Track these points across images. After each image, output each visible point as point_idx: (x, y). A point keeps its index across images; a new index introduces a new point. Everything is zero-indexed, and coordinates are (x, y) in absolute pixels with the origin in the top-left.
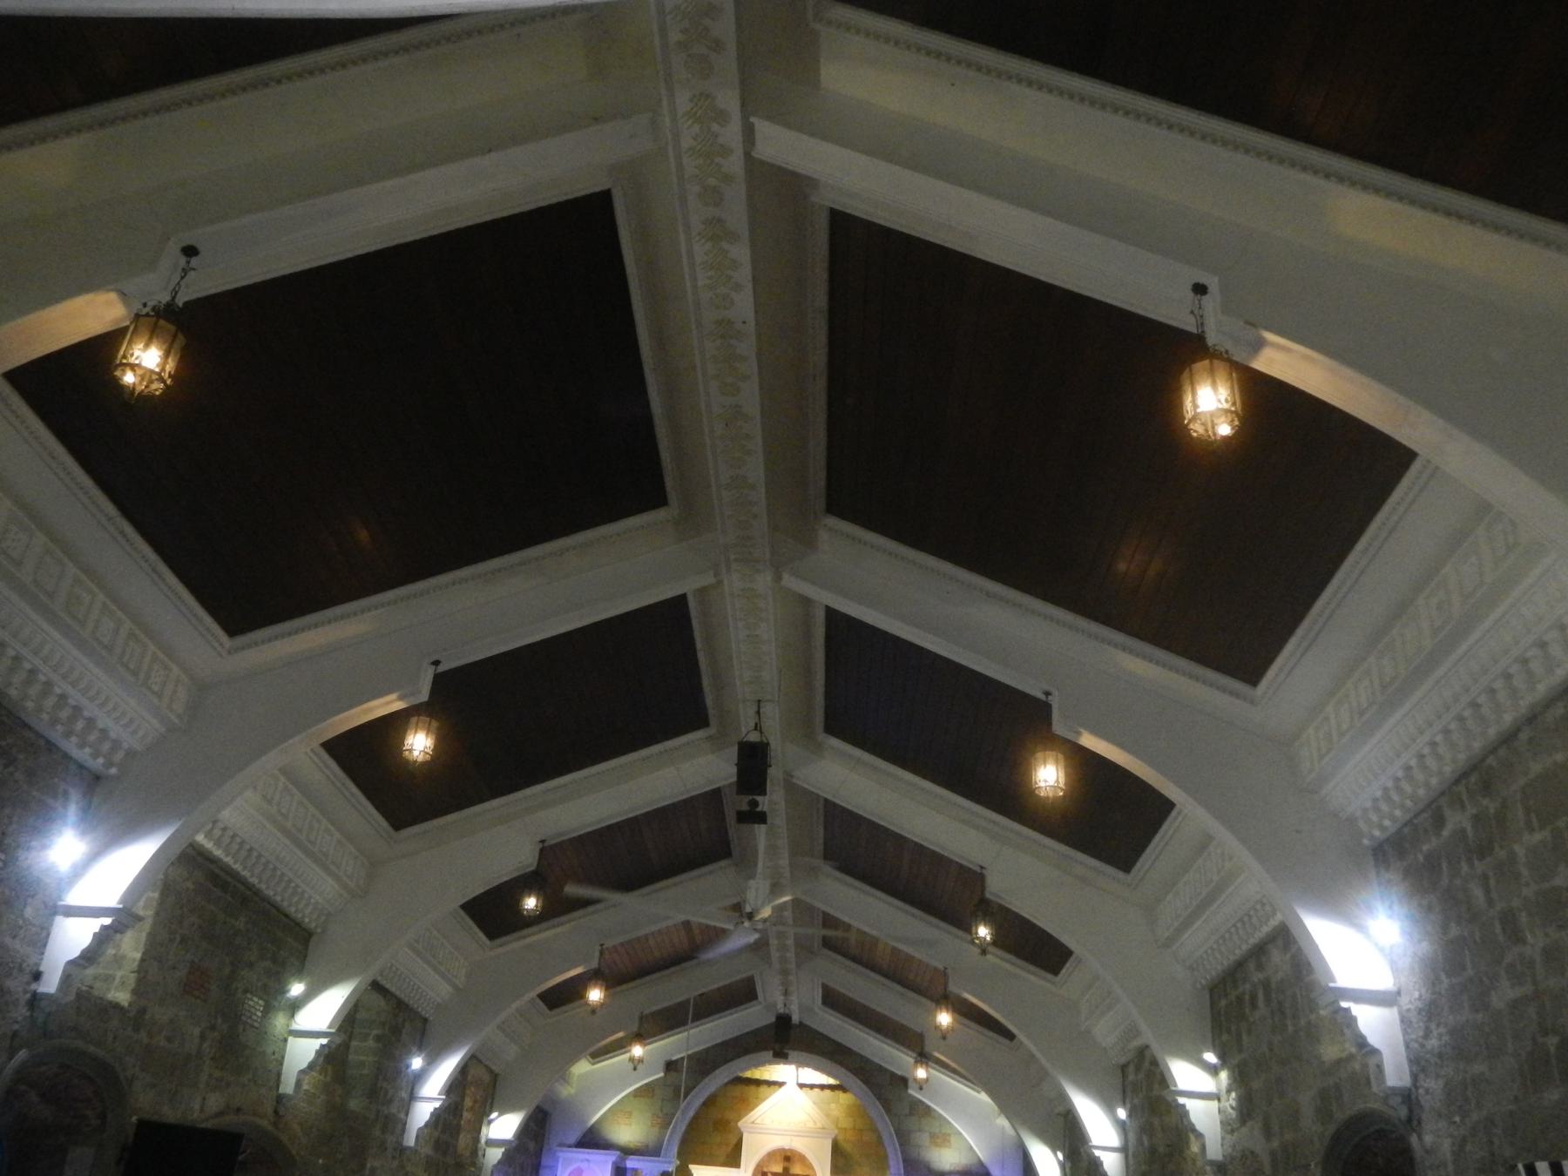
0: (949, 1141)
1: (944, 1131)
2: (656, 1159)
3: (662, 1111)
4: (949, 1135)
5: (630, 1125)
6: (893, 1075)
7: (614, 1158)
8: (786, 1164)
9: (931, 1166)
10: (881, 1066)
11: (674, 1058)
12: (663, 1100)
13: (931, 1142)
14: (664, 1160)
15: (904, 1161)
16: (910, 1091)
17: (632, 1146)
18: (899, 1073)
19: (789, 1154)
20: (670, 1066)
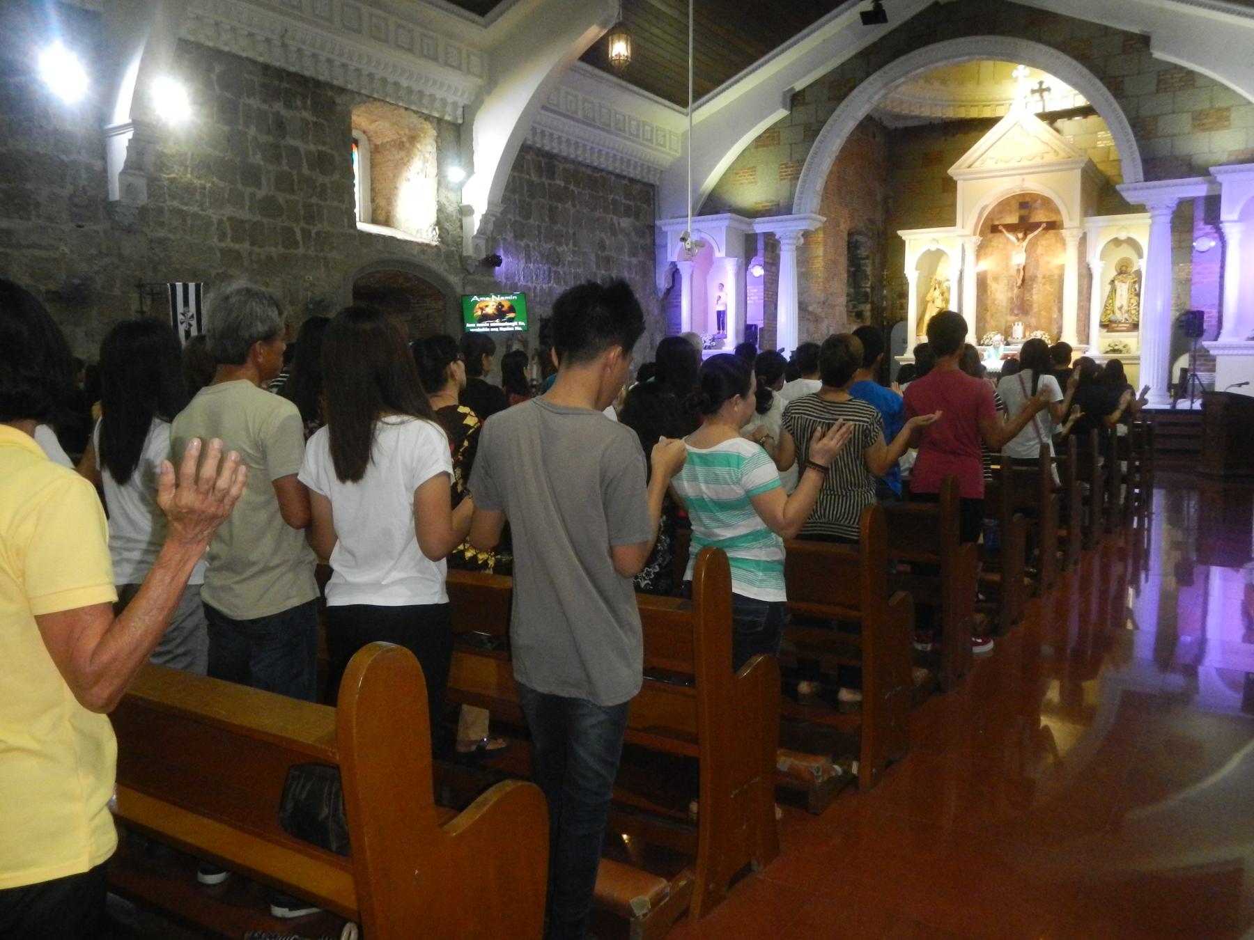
0: (1227, 119)
1: (1218, 105)
2: (789, 216)
3: (791, 160)
4: (1228, 109)
5: (756, 182)
6: (1128, 36)
7: (726, 223)
8: (1024, 212)
10: (1106, 28)
11: (799, 86)
12: (791, 144)
13: (1194, 126)
14: (797, 216)
16: (1157, 54)
17: (760, 207)
18: (1136, 30)
19: (1027, 199)
20: (795, 99)
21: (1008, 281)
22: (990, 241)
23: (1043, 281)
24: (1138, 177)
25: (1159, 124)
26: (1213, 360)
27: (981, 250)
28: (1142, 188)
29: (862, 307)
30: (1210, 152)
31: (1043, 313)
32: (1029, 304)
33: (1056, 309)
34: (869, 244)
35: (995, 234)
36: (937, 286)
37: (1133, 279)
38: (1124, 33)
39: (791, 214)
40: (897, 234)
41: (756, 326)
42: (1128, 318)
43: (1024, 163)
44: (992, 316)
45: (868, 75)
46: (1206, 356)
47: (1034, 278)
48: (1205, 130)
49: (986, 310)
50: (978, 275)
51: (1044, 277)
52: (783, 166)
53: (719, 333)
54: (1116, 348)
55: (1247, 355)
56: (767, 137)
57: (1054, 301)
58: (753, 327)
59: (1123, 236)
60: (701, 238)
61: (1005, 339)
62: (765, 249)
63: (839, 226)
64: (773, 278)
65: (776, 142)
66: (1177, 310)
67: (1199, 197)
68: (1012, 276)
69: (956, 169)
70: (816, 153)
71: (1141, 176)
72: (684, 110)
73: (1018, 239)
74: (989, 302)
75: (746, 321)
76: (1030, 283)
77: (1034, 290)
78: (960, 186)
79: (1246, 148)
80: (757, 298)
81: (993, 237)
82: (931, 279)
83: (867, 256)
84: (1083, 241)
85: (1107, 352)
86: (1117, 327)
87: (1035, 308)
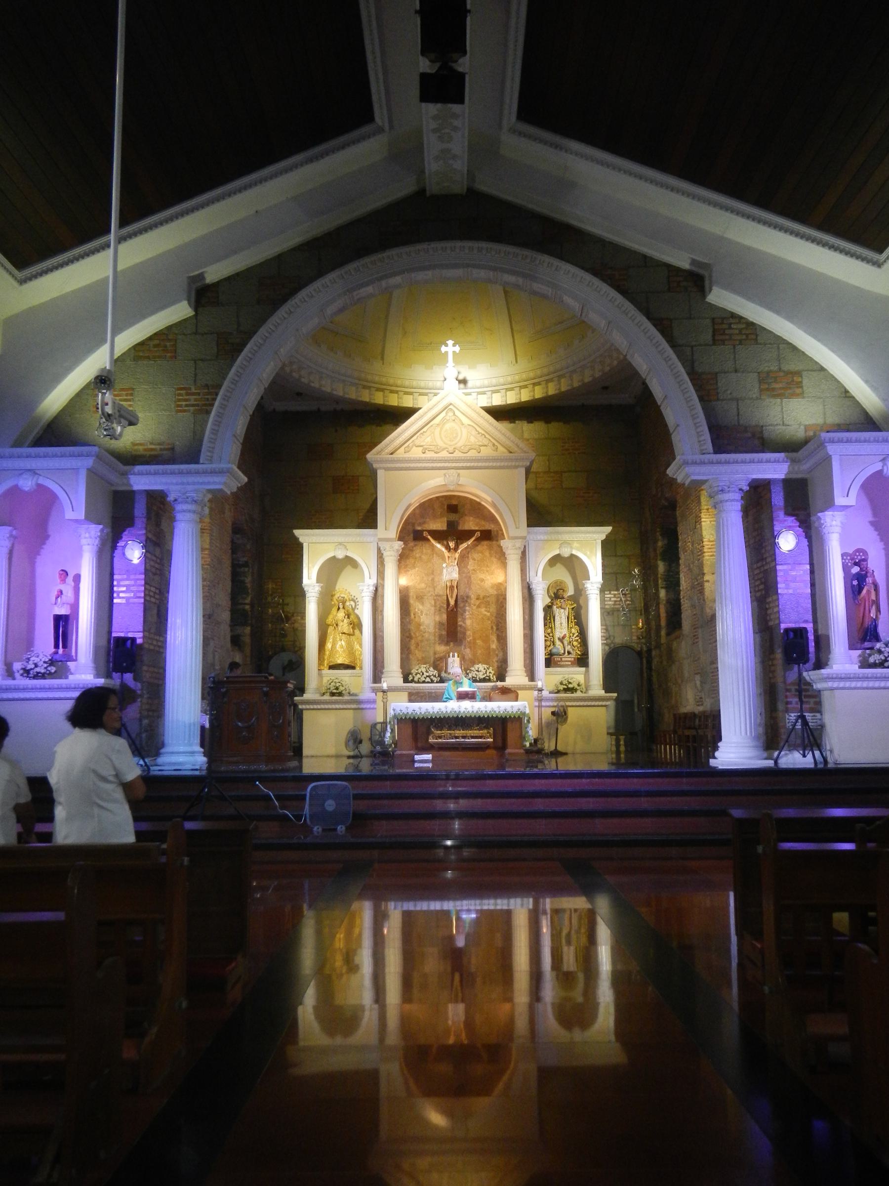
0: (799, 385)
1: (785, 368)
2: (193, 467)
3: (195, 381)
4: (799, 373)
7: (90, 462)
8: (453, 517)
9: (766, 435)
10: (645, 257)
12: (195, 361)
13: (761, 390)
15: (710, 429)
18: (685, 265)
19: (454, 502)
21: (435, 600)
22: (412, 551)
23: (478, 602)
24: (705, 447)
25: (720, 384)
26: (818, 694)
27: (403, 559)
28: (711, 463)
29: (239, 630)
30: (783, 424)
31: (479, 642)
32: (462, 630)
33: (494, 638)
34: (248, 547)
35: (420, 543)
36: (341, 607)
37: (572, 604)
38: (668, 266)
39: (197, 462)
40: (294, 534)
41: (133, 640)
42: (571, 651)
43: (457, 454)
44: (417, 645)
45: (320, 274)
46: (807, 690)
47: (466, 599)
48: (775, 396)
49: (410, 637)
50: (400, 591)
51: (477, 599)
52: (183, 392)
53: (56, 653)
54: (570, 686)
55: (867, 688)
56: (156, 346)
57: (492, 628)
58: (129, 642)
59: (566, 552)
60: (39, 486)
61: (439, 676)
62: (149, 518)
63: (224, 513)
64: (157, 566)
65: (169, 354)
66: (606, 644)
67: (775, 480)
68: (440, 596)
69: (378, 453)
70: (238, 375)
71: (709, 446)
72: (20, 275)
73: (448, 548)
74: (412, 627)
75: (110, 632)
76: (462, 605)
77: (467, 613)
78: (381, 474)
79: (825, 423)
80: (132, 595)
81: (415, 545)
82: (333, 596)
83: (246, 562)
84: (524, 554)
85: (558, 692)
86: (561, 661)
87: (468, 633)
